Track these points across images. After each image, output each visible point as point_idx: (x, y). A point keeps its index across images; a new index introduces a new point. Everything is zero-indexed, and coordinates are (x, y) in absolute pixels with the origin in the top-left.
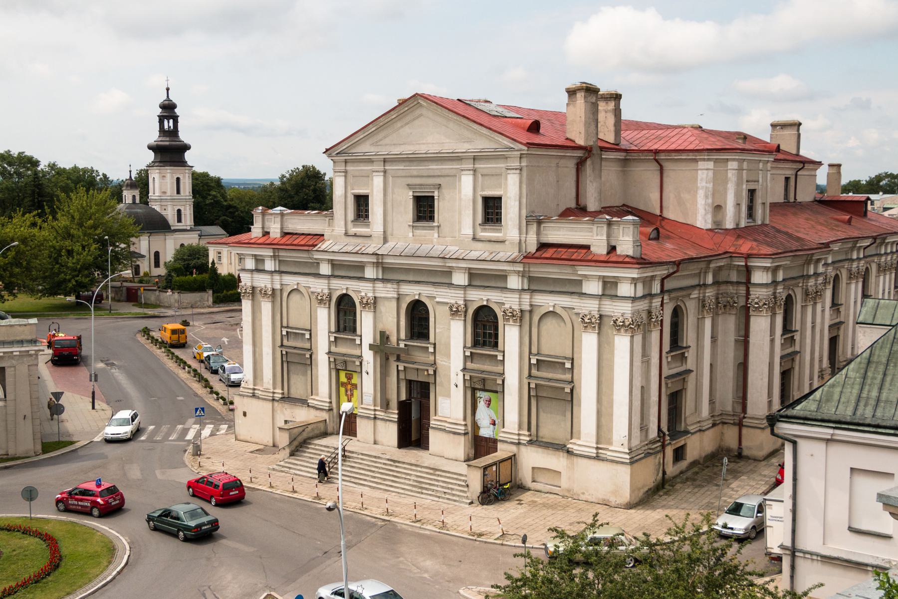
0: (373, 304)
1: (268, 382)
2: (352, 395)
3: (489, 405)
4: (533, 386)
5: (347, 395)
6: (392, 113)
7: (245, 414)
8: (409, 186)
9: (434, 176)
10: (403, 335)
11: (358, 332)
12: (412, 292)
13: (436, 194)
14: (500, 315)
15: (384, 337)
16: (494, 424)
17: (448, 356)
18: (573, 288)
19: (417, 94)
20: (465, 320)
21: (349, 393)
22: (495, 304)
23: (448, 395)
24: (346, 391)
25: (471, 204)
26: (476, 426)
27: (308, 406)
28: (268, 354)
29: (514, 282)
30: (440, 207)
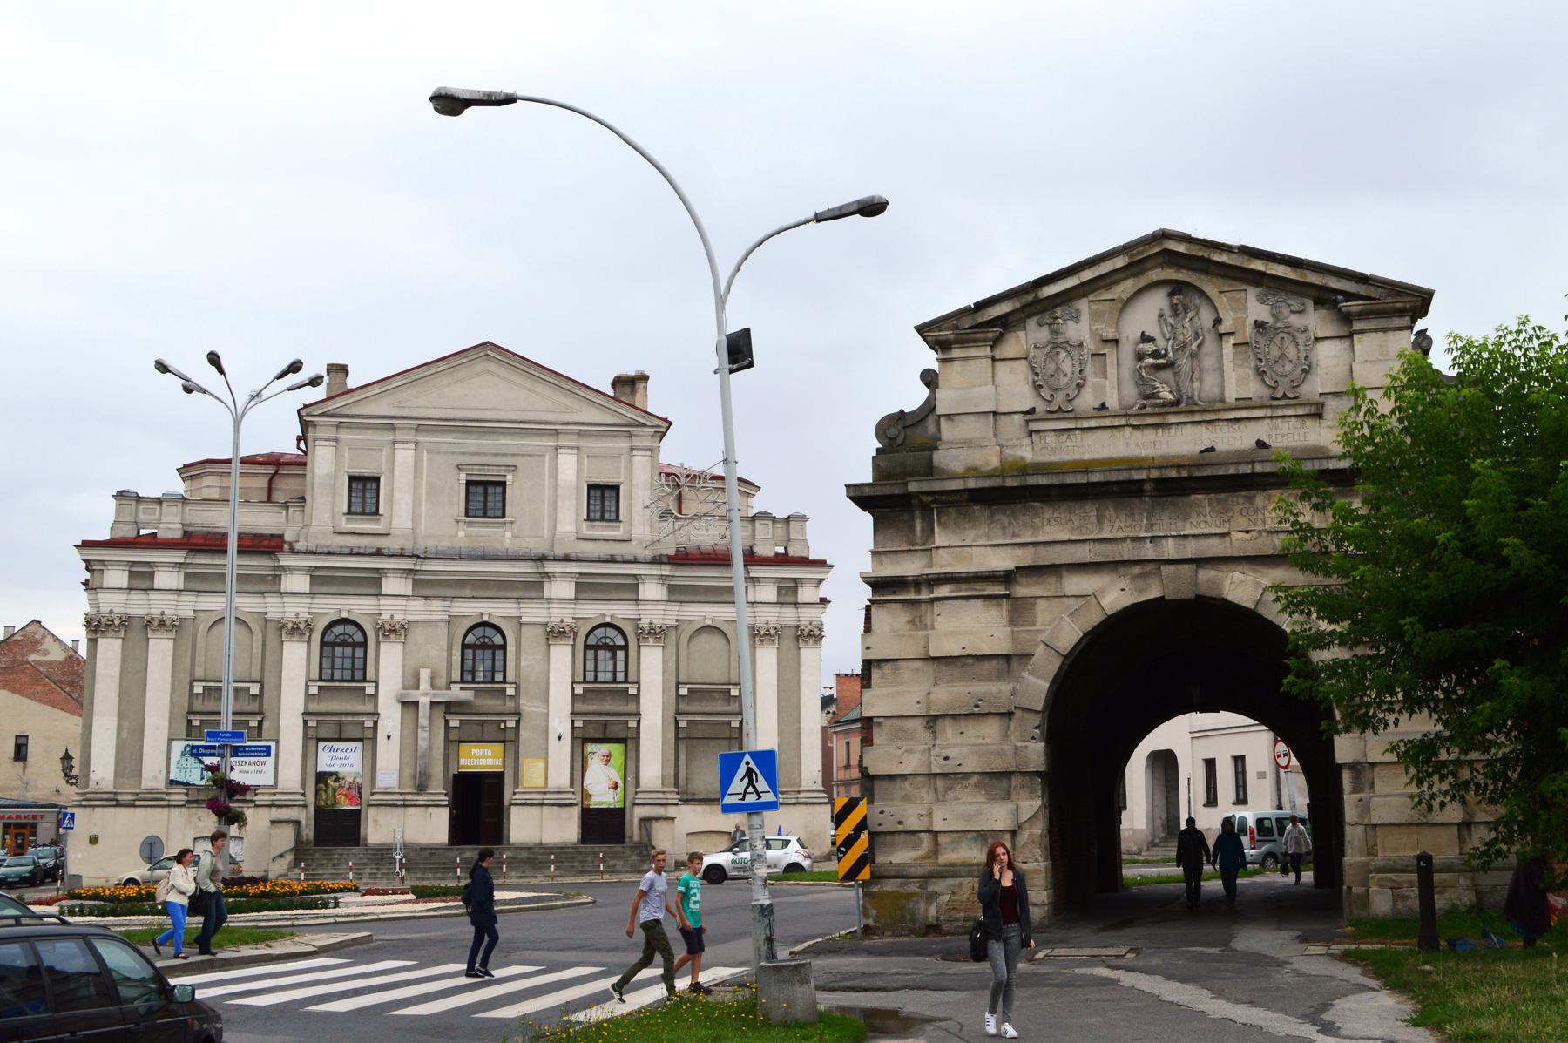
1: (155, 777)
3: (608, 761)
4: (683, 724)
6: (440, 363)
9: (505, 455)
10: (456, 675)
11: (370, 674)
12: (472, 609)
13: (509, 479)
16: (615, 787)
19: (488, 343)
20: (574, 646)
22: (627, 622)
25: (574, 492)
26: (585, 795)
27: (256, 806)
28: (157, 729)
29: (651, 591)
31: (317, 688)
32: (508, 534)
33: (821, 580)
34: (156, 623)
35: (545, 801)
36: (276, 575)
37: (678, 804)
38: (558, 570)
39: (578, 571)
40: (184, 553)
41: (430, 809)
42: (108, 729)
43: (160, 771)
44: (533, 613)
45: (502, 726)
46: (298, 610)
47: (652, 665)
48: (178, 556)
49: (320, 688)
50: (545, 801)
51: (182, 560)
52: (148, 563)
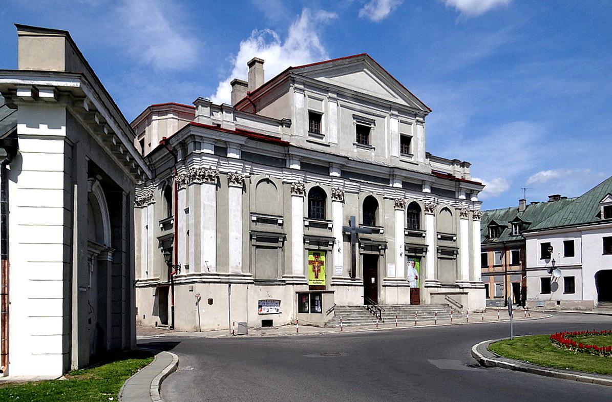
0: (338, 197)
1: (237, 266)
2: (319, 270)
3: (414, 266)
5: (314, 271)
7: (211, 302)
8: (355, 117)
14: (423, 209)
15: (351, 221)
16: (417, 279)
17: (393, 235)
18: (451, 194)
21: (316, 269)
23: (394, 262)
24: (314, 268)
27: (287, 284)
28: (237, 239)
29: (427, 190)
30: (373, 134)
31: (308, 222)
32: (373, 154)
33: (479, 191)
34: (234, 178)
35: (397, 284)
36: (284, 159)
37: (440, 287)
38: (399, 174)
39: (405, 175)
40: (245, 138)
41: (357, 287)
42: (211, 237)
43: (239, 264)
44: (387, 193)
45: (380, 247)
46: (299, 179)
47: (429, 223)
48: (241, 140)
49: (310, 223)
50: (397, 284)
51: (243, 143)
52: (226, 142)
